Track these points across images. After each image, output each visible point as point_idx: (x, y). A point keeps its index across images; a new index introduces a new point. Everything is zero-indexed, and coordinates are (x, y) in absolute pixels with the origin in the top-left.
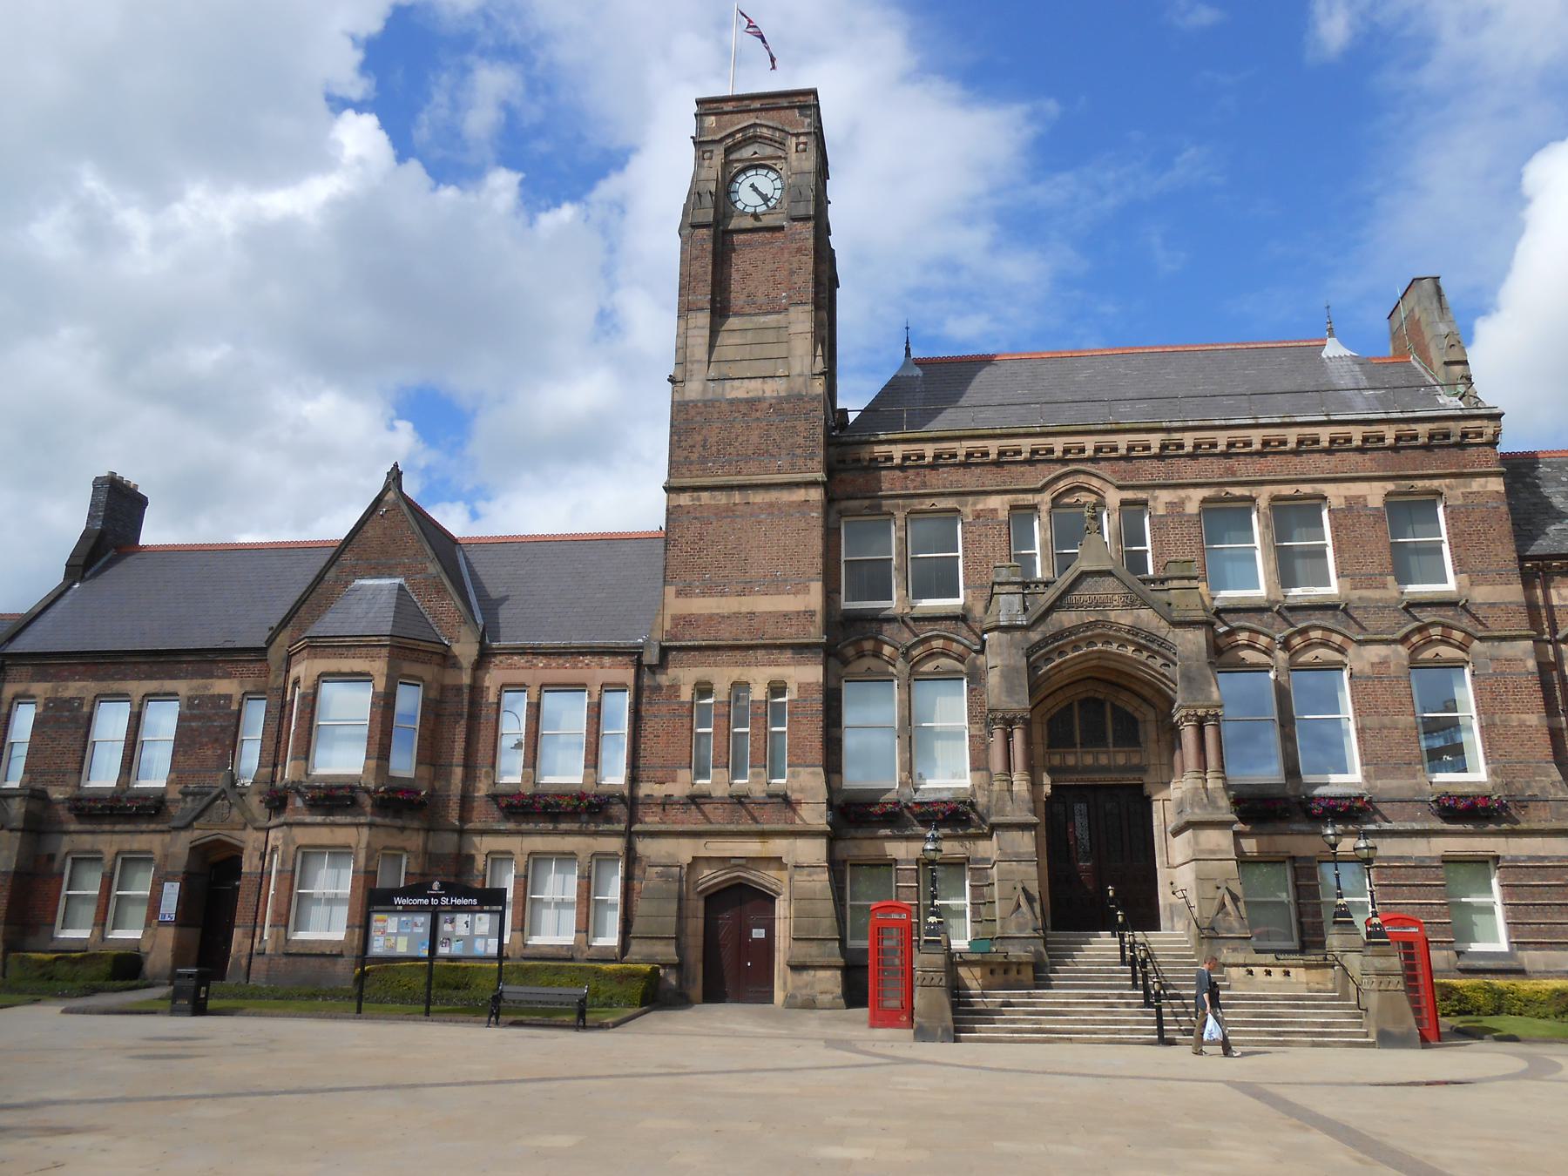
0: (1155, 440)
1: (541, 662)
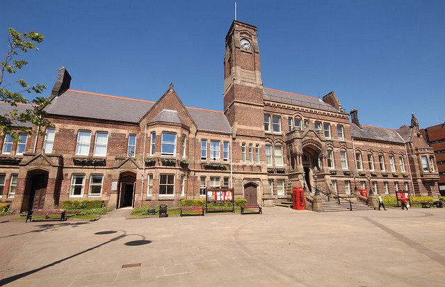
0: (309, 110)
1: (210, 134)
